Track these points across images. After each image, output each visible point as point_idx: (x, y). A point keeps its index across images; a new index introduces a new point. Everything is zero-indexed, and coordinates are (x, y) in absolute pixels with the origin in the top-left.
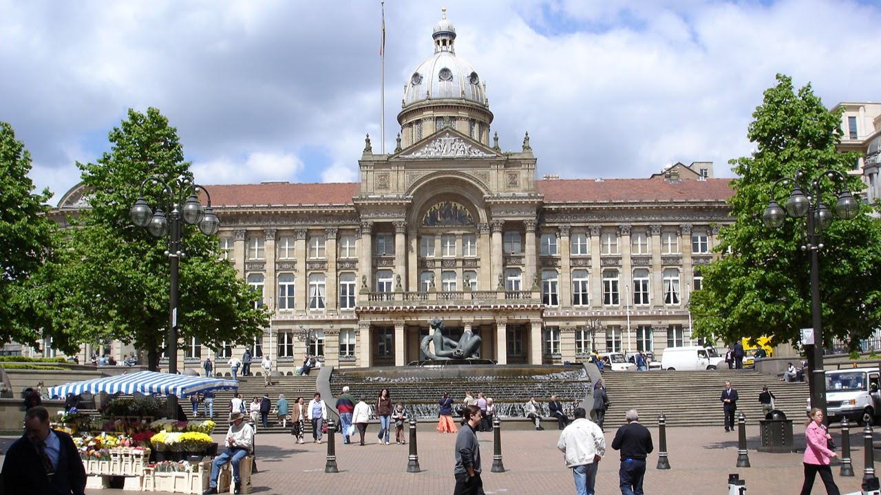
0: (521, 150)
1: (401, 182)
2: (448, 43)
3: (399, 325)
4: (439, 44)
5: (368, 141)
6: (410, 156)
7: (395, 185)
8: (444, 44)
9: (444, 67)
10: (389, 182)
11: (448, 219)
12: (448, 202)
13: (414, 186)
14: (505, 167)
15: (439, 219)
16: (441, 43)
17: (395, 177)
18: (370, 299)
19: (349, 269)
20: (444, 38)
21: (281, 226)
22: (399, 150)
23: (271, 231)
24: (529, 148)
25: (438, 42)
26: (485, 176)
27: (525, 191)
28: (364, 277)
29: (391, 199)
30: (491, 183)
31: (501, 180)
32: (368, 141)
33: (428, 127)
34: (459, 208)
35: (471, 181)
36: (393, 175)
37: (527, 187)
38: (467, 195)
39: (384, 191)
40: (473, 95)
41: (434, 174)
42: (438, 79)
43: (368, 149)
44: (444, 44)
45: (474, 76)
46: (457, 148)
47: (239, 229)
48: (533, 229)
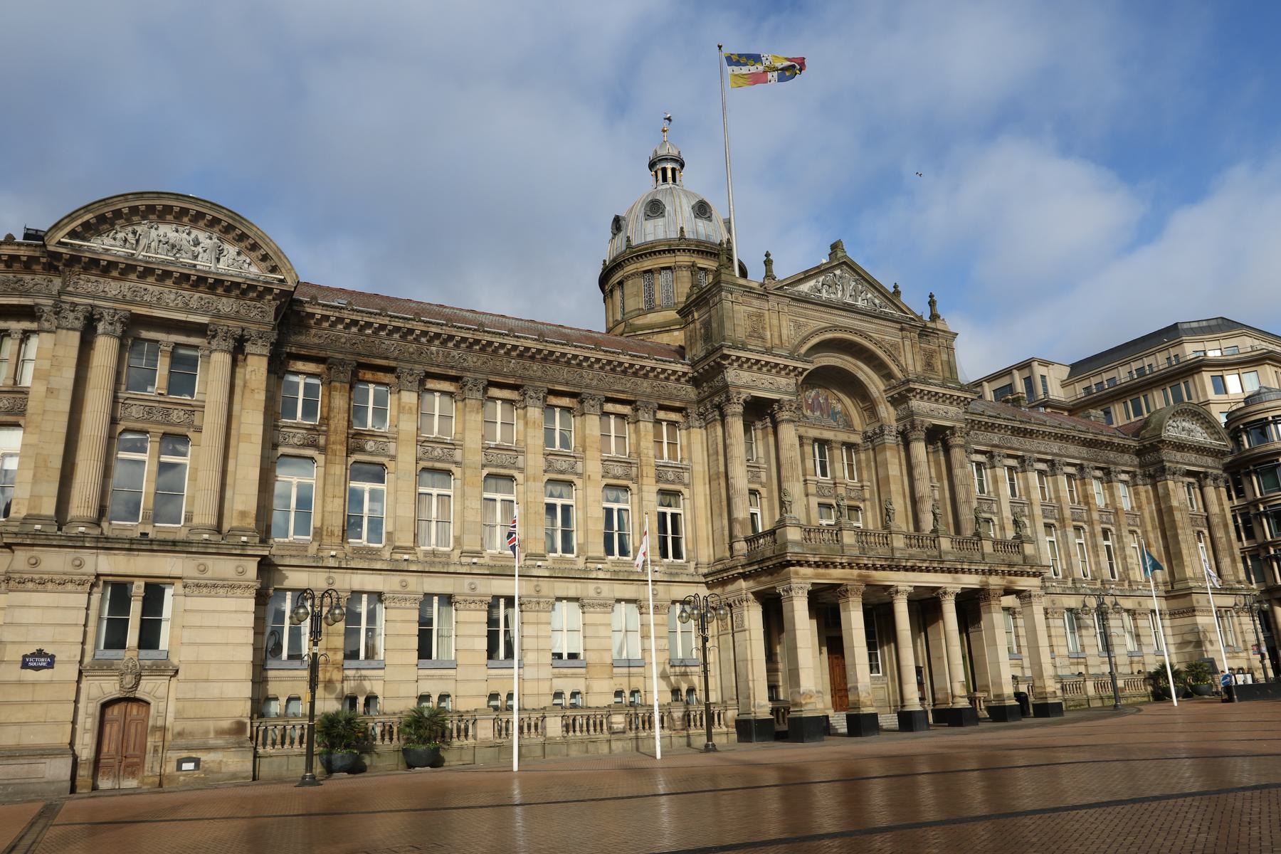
1: (785, 332)
7: (776, 335)
8: (665, 179)
10: (763, 328)
11: (818, 413)
14: (920, 335)
17: (775, 322)
36: (771, 319)
41: (825, 330)
44: (665, 179)
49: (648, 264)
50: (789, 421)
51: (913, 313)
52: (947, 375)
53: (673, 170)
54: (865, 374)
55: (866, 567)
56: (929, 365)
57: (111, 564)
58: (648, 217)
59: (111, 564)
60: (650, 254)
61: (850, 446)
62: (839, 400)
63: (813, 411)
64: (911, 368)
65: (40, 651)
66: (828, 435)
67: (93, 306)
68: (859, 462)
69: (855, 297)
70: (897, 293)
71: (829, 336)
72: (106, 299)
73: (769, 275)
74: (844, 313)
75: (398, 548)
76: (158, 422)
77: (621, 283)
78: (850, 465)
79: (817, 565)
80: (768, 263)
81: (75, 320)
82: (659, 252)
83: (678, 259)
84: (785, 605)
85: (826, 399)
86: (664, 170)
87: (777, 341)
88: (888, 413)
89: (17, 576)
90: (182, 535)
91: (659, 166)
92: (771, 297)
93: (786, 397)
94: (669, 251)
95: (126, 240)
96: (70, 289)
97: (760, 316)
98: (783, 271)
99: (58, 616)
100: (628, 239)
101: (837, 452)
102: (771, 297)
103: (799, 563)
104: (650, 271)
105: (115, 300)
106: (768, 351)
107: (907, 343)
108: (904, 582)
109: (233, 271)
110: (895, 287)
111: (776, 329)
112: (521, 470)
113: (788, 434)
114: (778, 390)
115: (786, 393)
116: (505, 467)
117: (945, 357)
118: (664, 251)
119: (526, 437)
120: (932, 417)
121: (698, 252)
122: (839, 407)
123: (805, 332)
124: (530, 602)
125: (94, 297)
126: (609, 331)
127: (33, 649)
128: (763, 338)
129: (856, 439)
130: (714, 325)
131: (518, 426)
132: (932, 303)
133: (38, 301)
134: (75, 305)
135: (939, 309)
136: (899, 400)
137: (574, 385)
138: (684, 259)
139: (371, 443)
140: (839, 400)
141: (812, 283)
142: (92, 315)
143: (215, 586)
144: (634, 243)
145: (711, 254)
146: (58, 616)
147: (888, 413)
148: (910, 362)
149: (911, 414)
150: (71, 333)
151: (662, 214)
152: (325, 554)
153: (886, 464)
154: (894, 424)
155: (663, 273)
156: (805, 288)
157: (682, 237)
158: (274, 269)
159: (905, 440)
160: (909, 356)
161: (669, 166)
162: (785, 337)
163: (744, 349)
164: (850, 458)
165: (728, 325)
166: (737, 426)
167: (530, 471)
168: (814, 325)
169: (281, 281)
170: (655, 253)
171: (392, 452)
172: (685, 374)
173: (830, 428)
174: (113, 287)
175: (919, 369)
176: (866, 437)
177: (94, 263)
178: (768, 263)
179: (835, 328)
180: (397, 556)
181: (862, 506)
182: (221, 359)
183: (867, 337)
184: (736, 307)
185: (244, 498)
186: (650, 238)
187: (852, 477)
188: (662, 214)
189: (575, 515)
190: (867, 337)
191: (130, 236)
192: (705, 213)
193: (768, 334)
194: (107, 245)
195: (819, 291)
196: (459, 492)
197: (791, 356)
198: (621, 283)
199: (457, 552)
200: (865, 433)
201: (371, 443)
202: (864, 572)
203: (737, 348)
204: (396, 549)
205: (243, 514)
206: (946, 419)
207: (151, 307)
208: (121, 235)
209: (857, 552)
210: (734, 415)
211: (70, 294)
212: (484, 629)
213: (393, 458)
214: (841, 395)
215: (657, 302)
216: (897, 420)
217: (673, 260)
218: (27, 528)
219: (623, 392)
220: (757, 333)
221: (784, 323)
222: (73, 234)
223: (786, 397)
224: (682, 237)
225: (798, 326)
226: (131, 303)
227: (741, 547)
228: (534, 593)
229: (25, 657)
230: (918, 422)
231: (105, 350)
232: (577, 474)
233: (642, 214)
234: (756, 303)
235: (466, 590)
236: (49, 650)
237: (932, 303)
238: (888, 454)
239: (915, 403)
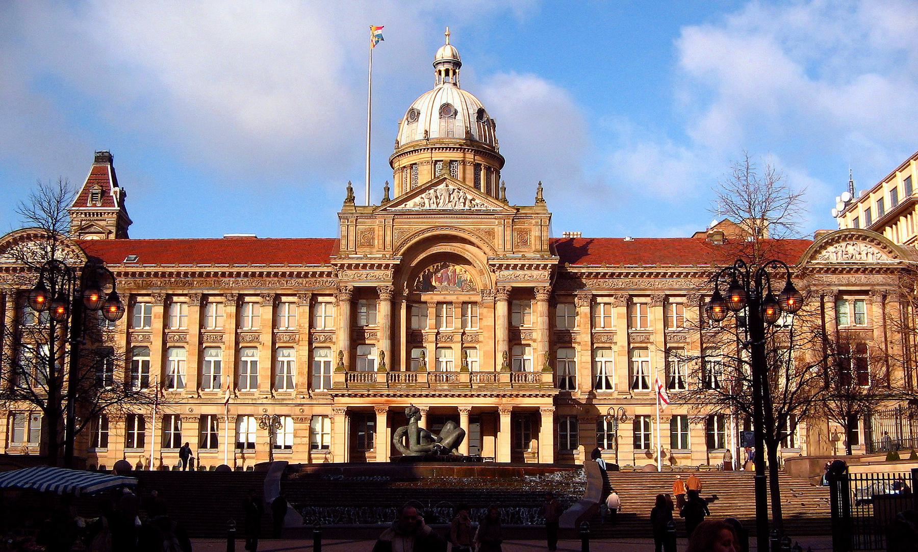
0: (532, 203)
1: (388, 239)
2: (451, 73)
5: (350, 190)
6: (400, 208)
7: (381, 242)
9: (444, 102)
10: (373, 238)
12: (445, 264)
13: (402, 245)
15: (434, 284)
16: (443, 73)
17: (381, 233)
18: (346, 380)
19: (324, 342)
20: (447, 66)
21: (242, 289)
22: (387, 200)
23: (232, 295)
24: (542, 200)
26: (490, 233)
27: (536, 251)
28: (341, 352)
29: (375, 258)
30: (496, 241)
31: (508, 238)
33: (426, 172)
34: (458, 271)
35: (473, 239)
36: (379, 232)
37: (539, 247)
38: (467, 256)
39: (367, 250)
40: (480, 136)
41: (428, 230)
43: (351, 199)
45: (481, 113)
46: (456, 199)
47: (193, 292)
48: (545, 297)
63: (441, 283)
97: (372, 231)
138: (426, 155)
156: (410, 205)
167: (227, 343)
175: (508, 246)
183: (461, 230)
190: (461, 230)
197: (384, 257)
206: (528, 281)
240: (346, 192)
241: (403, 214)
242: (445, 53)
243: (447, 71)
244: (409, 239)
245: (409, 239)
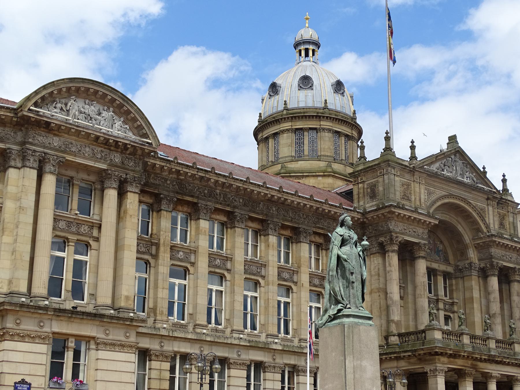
1: (423, 197)
3: (470, 375)
4: (300, 55)
5: (387, 139)
7: (418, 198)
8: (307, 55)
10: (410, 193)
14: (498, 203)
16: (303, 53)
20: (307, 46)
22: (413, 157)
25: (300, 51)
32: (387, 139)
33: (327, 139)
41: (445, 197)
42: (297, 89)
44: (307, 55)
49: (299, 125)
50: (423, 258)
51: (495, 188)
52: (512, 232)
53: (313, 51)
54: (462, 228)
55: (476, 359)
56: (502, 225)
57: (59, 327)
58: (300, 88)
59: (59, 327)
60: (302, 117)
61: (446, 276)
62: (441, 242)
64: (492, 226)
65: (23, 380)
66: (435, 266)
67: (45, 153)
68: (451, 285)
69: (462, 175)
70: (485, 173)
71: (446, 201)
72: (51, 149)
73: (413, 157)
74: (456, 186)
75: (199, 325)
76: (73, 233)
77: (275, 135)
78: (445, 288)
79: (451, 356)
80: (413, 148)
81: (32, 162)
82: (309, 116)
83: (322, 123)
84: (431, 381)
85: (434, 241)
86: (307, 50)
87: (418, 203)
88: (473, 255)
89: (10, 330)
90: (90, 309)
91: (302, 47)
92: (416, 173)
93: (423, 242)
94: (316, 116)
95: (61, 109)
96: (30, 140)
97: (408, 185)
98: (421, 154)
99: (31, 358)
100: (285, 104)
101: (439, 277)
102: (416, 173)
103: (442, 354)
104: (301, 129)
105: (56, 150)
106: (416, 211)
107: (491, 208)
108: (496, 371)
109: (121, 134)
110: (484, 168)
111: (418, 195)
112: (263, 277)
113: (422, 266)
114: (418, 237)
115: (423, 239)
116: (254, 275)
117: (511, 219)
118: (313, 116)
119: (268, 255)
120: (503, 260)
121: (336, 119)
122: (441, 247)
123: (434, 197)
124: (270, 366)
125: (44, 147)
126: (262, 167)
127: (18, 379)
128: (409, 200)
129: (450, 269)
130: (381, 189)
131: (261, 246)
132: (504, 181)
133: (8, 146)
134: (35, 151)
135: (509, 186)
136: (483, 247)
137: (295, 223)
138: (326, 124)
139: (181, 253)
140: (441, 242)
141: (437, 165)
142: (44, 159)
143: (114, 345)
144: (289, 106)
145: (345, 121)
146: (31, 358)
147: (473, 255)
148: (491, 221)
149: (491, 257)
150: (32, 170)
151: (311, 87)
152: (159, 325)
153: (471, 289)
154: (477, 262)
155: (310, 132)
157: (325, 108)
158: (145, 136)
159: (484, 274)
160: (491, 217)
161: (311, 47)
162: (422, 201)
163: (403, 208)
164: (445, 283)
165: (392, 190)
166: (394, 259)
167: (271, 278)
168: (439, 193)
169: (150, 144)
170: (306, 116)
171: (193, 260)
172: (359, 219)
173: (436, 261)
174: (56, 142)
176: (458, 270)
177: (48, 124)
178: (413, 148)
179: (450, 196)
180: (198, 330)
181: (452, 315)
182: (111, 195)
184: (397, 179)
185: (129, 288)
186: (302, 105)
187: (446, 296)
188: (311, 87)
189: (291, 310)
190: (469, 204)
191: (63, 106)
192: (340, 90)
193: (413, 197)
194: (53, 113)
195: (443, 170)
196: (228, 290)
197: (428, 215)
198: (275, 135)
199: (229, 330)
200: (458, 266)
201: (181, 253)
202: (474, 363)
203: (399, 207)
204: (196, 326)
205: (127, 298)
207: (75, 156)
208: (59, 105)
209: (470, 349)
210: (393, 251)
211: (31, 144)
212: (244, 382)
213: (193, 264)
214: (443, 238)
215: (306, 153)
216: (479, 260)
217: (318, 123)
218: (15, 300)
219: (322, 229)
220: (406, 197)
221: (423, 191)
222: (36, 104)
223: (423, 242)
224: (325, 108)
225: (430, 194)
226: (64, 152)
227: (394, 340)
228: (271, 360)
229: (15, 383)
230: (495, 263)
231: (50, 182)
232: (294, 282)
233: (297, 85)
234: (407, 176)
235: (235, 356)
236: (28, 379)
237: (504, 181)
238: (473, 283)
239: (495, 251)
240: (384, 142)
241: (434, 176)
242: (308, 33)
243: (307, 50)
244: (434, 202)
245: (434, 202)
